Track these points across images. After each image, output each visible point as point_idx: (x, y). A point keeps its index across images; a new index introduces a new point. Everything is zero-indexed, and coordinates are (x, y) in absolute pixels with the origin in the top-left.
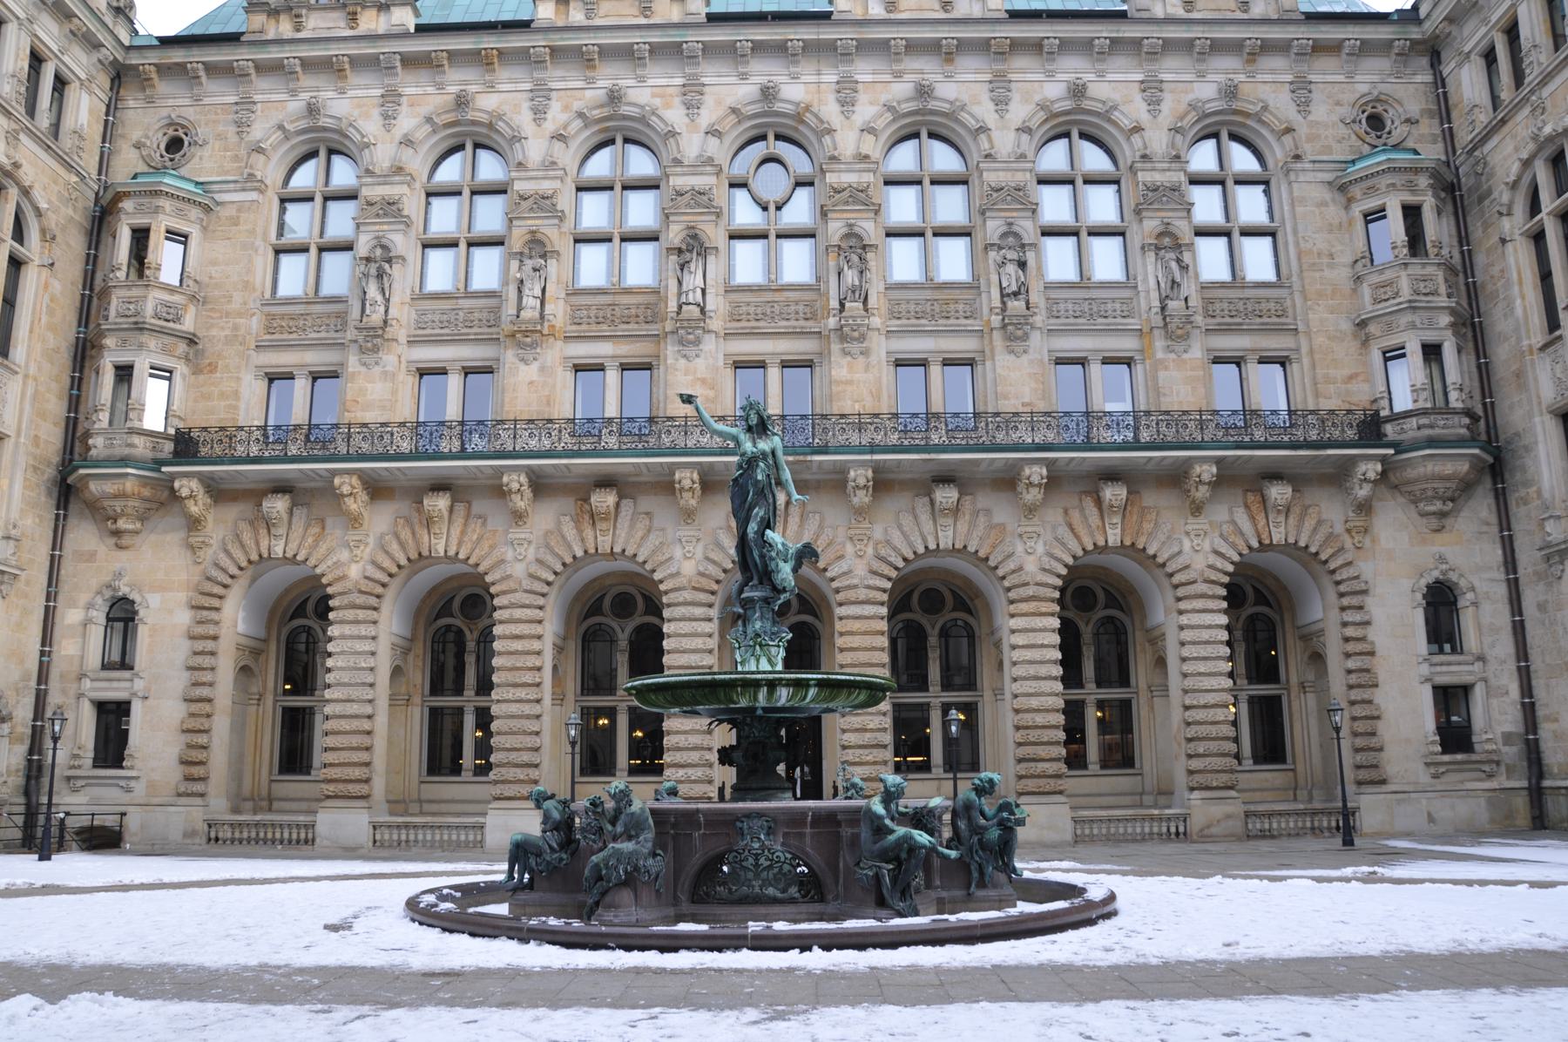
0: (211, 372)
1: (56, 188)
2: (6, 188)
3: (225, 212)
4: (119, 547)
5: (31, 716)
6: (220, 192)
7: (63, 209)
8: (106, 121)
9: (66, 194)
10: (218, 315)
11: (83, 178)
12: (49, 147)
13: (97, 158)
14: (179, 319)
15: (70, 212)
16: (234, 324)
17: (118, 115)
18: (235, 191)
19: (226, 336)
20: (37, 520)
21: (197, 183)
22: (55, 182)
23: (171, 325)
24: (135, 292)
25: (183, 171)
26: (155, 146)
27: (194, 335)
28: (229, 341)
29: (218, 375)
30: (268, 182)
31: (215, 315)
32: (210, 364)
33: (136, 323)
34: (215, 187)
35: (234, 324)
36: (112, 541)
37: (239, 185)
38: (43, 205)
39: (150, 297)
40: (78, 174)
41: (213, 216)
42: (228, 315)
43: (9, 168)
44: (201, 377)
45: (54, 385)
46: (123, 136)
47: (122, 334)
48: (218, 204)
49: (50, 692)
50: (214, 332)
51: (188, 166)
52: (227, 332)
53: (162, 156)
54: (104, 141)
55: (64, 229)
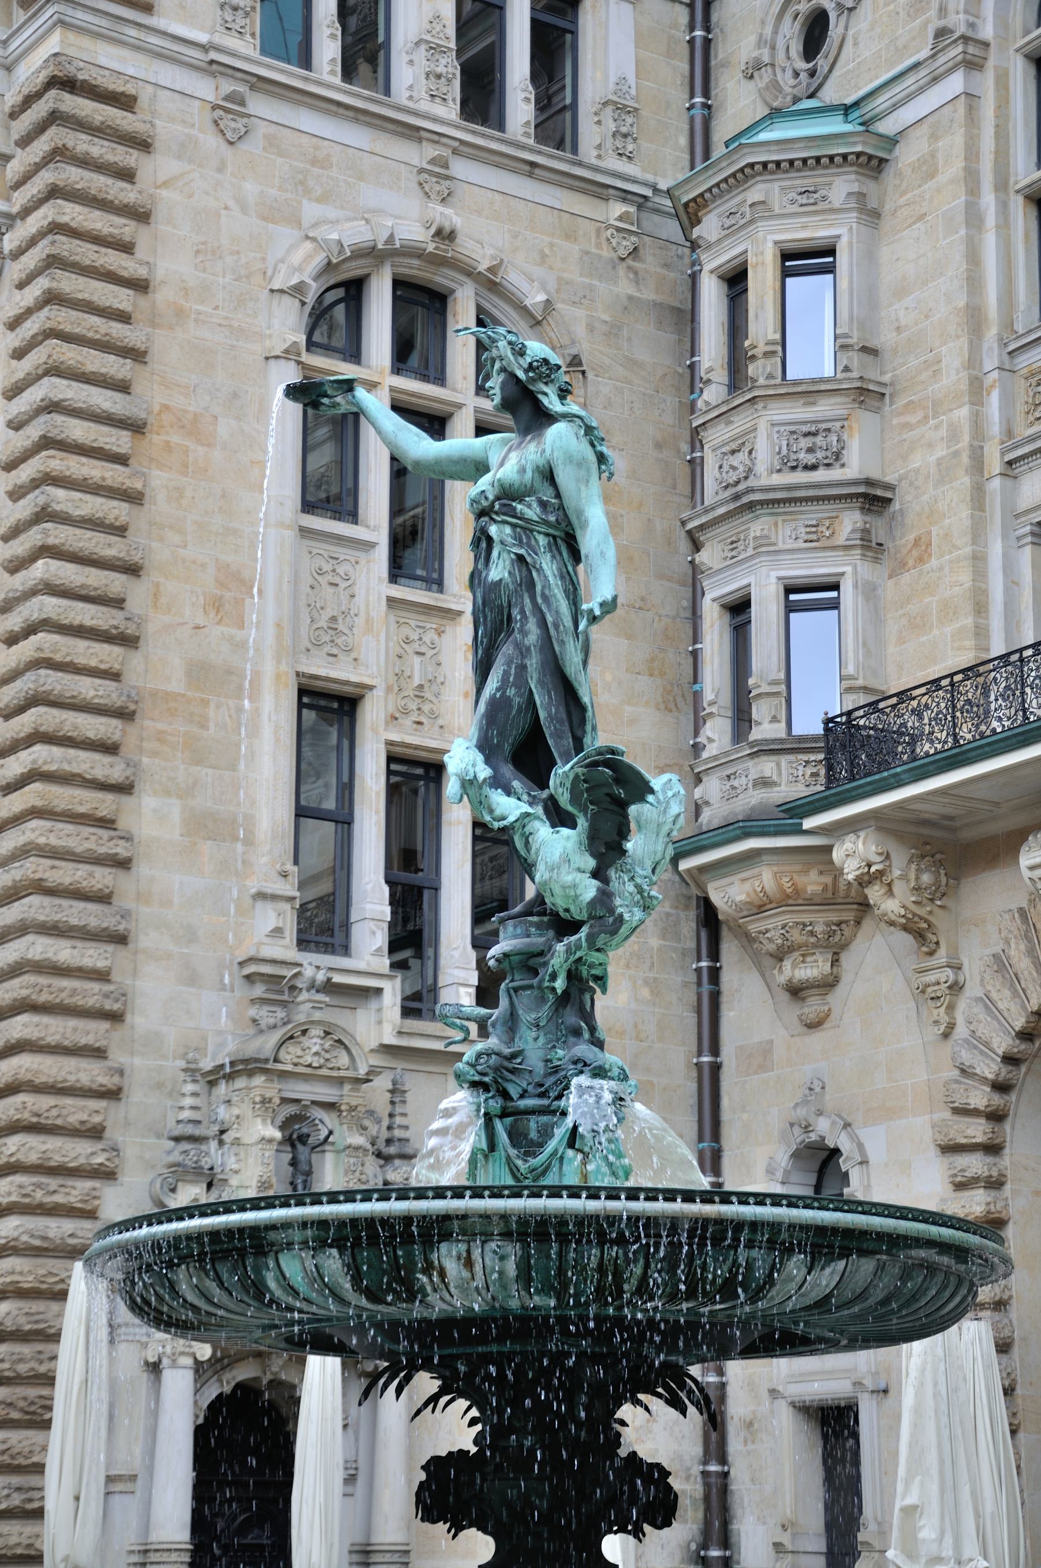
0: (921, 560)
1: (574, 249)
2: (453, 291)
3: (906, 156)
4: (813, 1025)
5: (698, 1450)
6: (895, 107)
7: (601, 286)
8: (691, 42)
9: (606, 253)
10: (919, 415)
11: (642, 202)
12: (533, 165)
13: (683, 141)
14: (838, 456)
15: (625, 287)
16: (951, 425)
17: (714, 18)
18: (921, 90)
19: (939, 462)
20: (645, 993)
21: (847, 110)
22: (569, 236)
23: (821, 475)
24: (740, 423)
25: (830, 94)
26: (781, 55)
27: (869, 482)
28: (944, 473)
29: (934, 563)
30: (987, 31)
31: (913, 419)
32: (917, 542)
33: (737, 497)
34: (882, 101)
35: (951, 425)
36: (793, 1012)
37: (923, 72)
38: (535, 298)
39: (763, 426)
40: (625, 196)
41: (889, 174)
42: (937, 408)
43: (431, 248)
44: (906, 578)
45: (644, 683)
46: (725, 64)
47: (726, 530)
48: (892, 141)
49: (730, 1390)
50: (917, 461)
51: (836, 73)
52: (941, 452)
53: (796, 74)
54: (692, 96)
55: (613, 331)
